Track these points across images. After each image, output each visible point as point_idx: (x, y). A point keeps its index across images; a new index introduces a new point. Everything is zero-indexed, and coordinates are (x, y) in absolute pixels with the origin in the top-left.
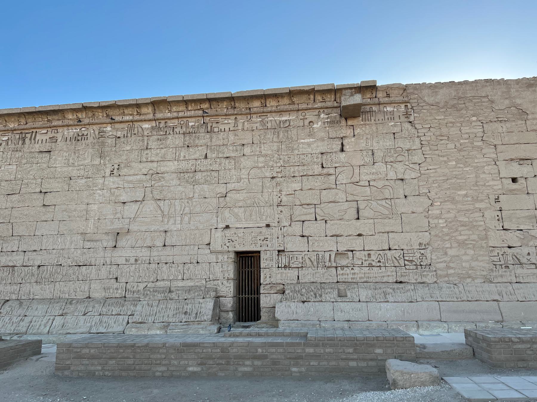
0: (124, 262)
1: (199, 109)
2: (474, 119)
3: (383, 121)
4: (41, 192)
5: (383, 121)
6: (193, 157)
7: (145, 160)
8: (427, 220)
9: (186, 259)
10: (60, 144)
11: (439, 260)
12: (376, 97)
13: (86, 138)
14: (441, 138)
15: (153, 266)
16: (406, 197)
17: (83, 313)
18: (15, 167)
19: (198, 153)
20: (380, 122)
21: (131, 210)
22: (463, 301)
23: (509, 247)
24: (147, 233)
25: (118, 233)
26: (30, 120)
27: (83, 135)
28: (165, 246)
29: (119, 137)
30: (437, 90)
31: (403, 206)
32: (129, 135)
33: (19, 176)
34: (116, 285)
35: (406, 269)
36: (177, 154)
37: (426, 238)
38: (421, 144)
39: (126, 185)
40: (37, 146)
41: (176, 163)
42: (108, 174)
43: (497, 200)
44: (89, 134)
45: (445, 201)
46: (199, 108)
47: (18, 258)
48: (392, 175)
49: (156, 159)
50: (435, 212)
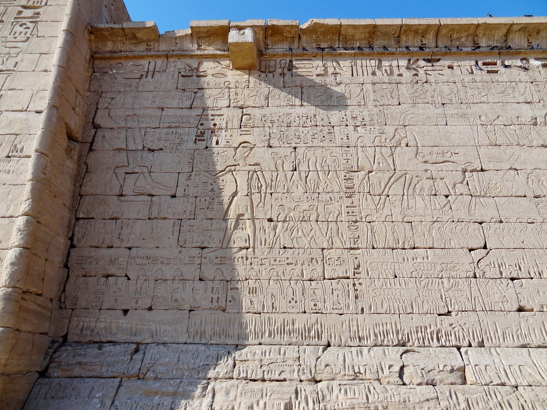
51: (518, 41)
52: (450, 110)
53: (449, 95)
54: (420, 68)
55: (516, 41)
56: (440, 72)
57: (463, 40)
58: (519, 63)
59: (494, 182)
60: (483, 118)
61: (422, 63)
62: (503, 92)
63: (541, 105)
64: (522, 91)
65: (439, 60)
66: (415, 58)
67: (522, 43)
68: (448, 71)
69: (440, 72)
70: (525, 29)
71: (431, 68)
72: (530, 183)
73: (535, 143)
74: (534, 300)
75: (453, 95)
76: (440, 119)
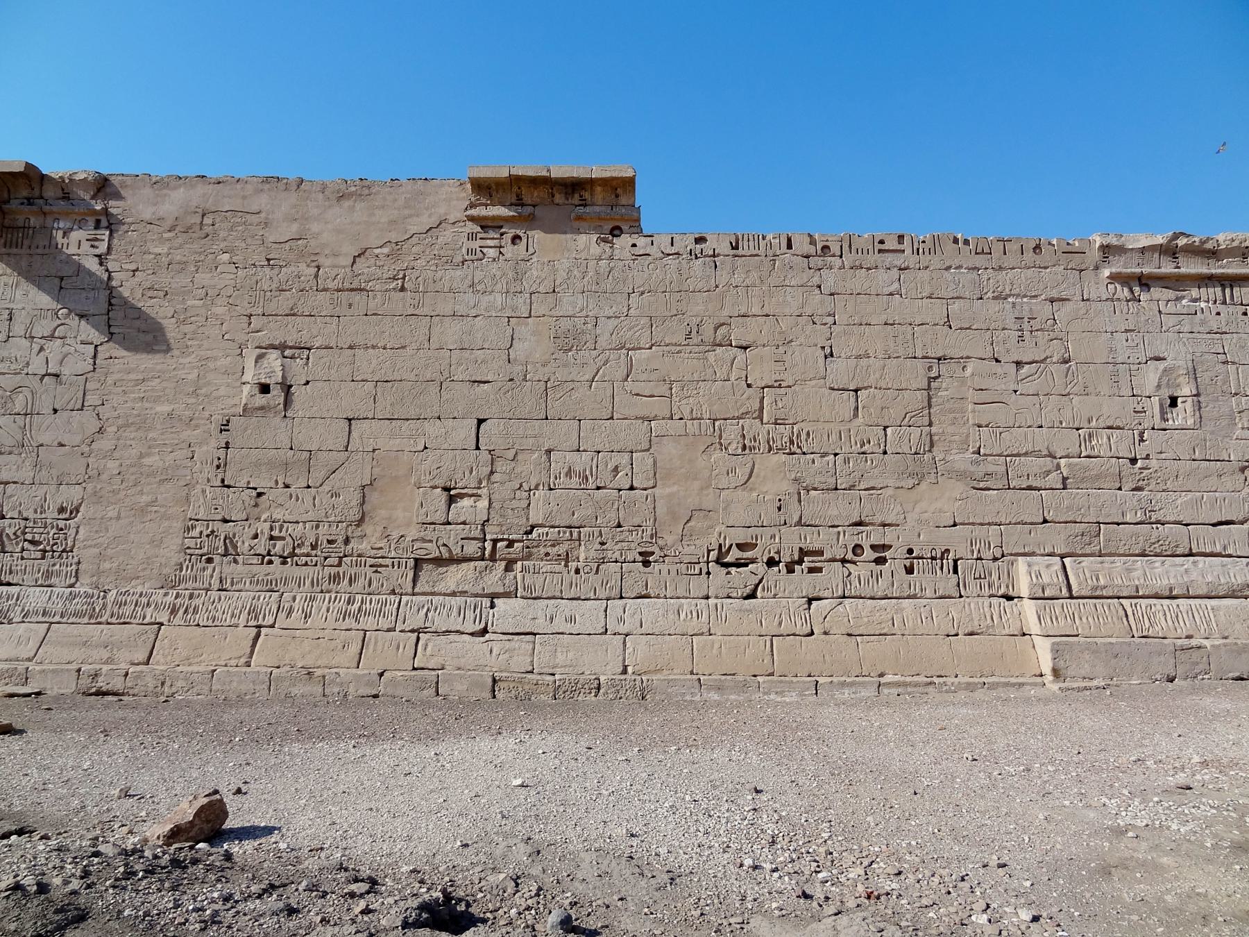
2: (226, 257)
3: (47, 251)
5: (47, 251)
8: (83, 461)
11: (90, 543)
12: (42, 198)
14: (150, 293)
16: (55, 411)
20: (39, 251)
22: (100, 623)
23: (225, 521)
30: (165, 191)
31: (47, 431)
35: (23, 558)
37: (71, 495)
38: (110, 304)
43: (225, 427)
45: (128, 426)
48: (37, 366)
50: (104, 444)
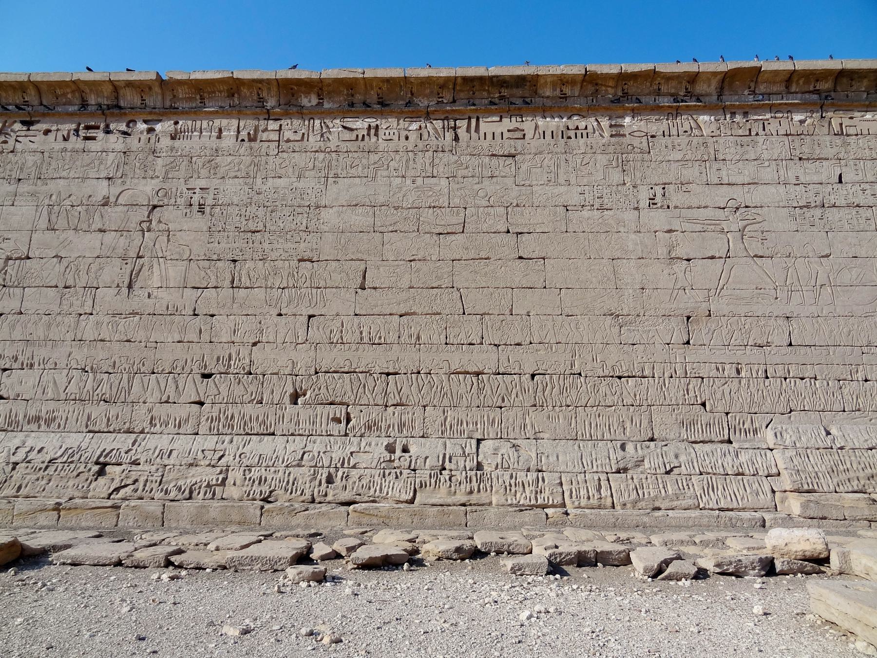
0: (714, 373)
1: (810, 92)
4: (508, 232)
6: (816, 179)
7: (716, 181)
9: (840, 371)
10: (533, 143)
13: (585, 135)
15: (774, 384)
17: (663, 470)
18: (444, 182)
19: (828, 171)
21: (704, 273)
24: (749, 320)
25: (688, 318)
26: (462, 95)
27: (577, 128)
28: (790, 345)
29: (653, 136)
32: (674, 132)
33: (456, 201)
34: (705, 417)
36: (781, 172)
39: (687, 226)
40: (485, 144)
41: (781, 189)
42: (644, 203)
44: (590, 127)
46: (812, 88)
47: (484, 356)
49: (739, 179)
51: (129, 98)
52: (24, 188)
53: (30, 168)
54: (15, 132)
55: (129, 98)
56: (32, 139)
57: (69, 96)
58: (123, 127)
59: (32, 271)
60: (54, 197)
61: (17, 126)
62: (87, 166)
63: (120, 181)
64: (109, 163)
65: (38, 122)
66: (12, 120)
67: (135, 101)
68: (40, 137)
69: (32, 139)
70: (129, 84)
71: (23, 133)
72: (68, 270)
73: (93, 227)
74: (13, 389)
75: (34, 168)
76: (8, 198)
